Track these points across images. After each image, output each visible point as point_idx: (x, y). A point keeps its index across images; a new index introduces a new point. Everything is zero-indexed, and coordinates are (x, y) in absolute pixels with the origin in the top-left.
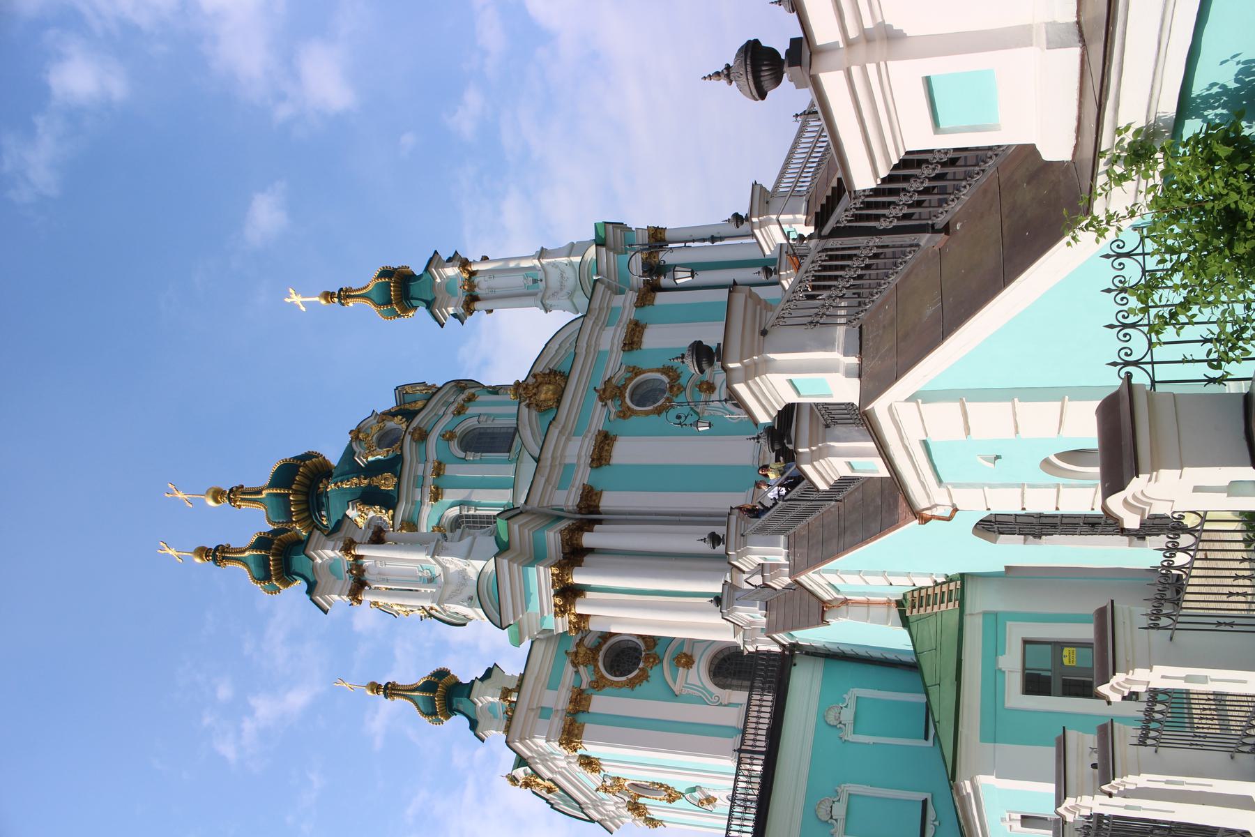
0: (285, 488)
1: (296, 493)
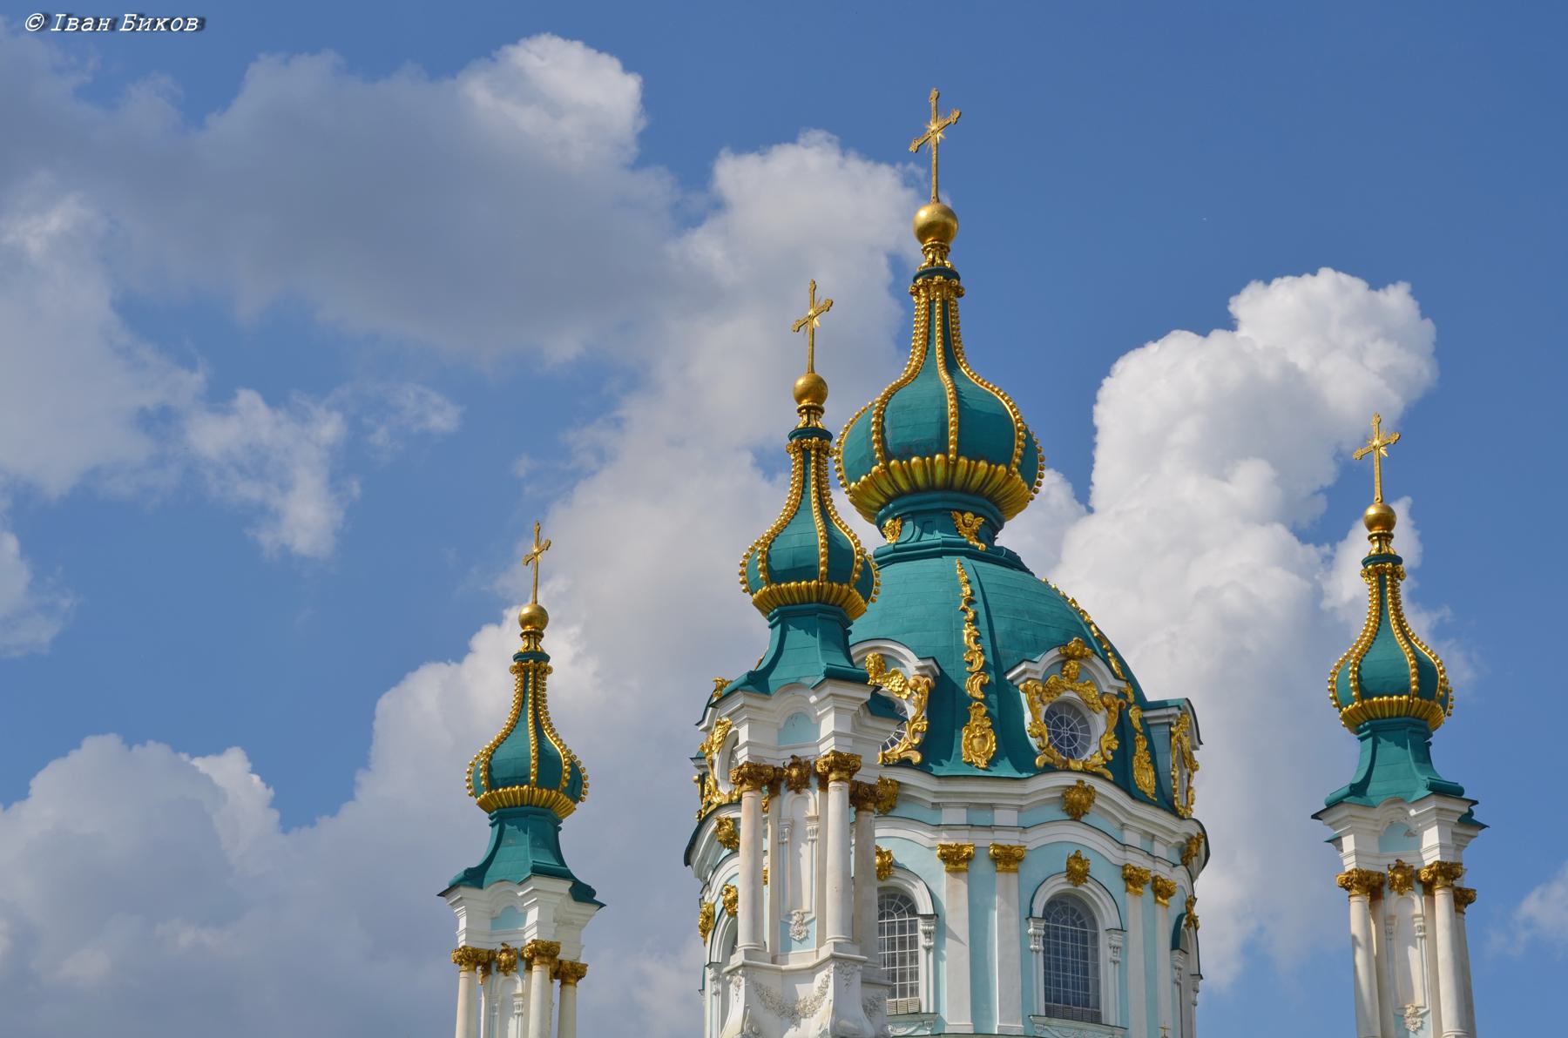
0: (959, 443)
1: (951, 466)
